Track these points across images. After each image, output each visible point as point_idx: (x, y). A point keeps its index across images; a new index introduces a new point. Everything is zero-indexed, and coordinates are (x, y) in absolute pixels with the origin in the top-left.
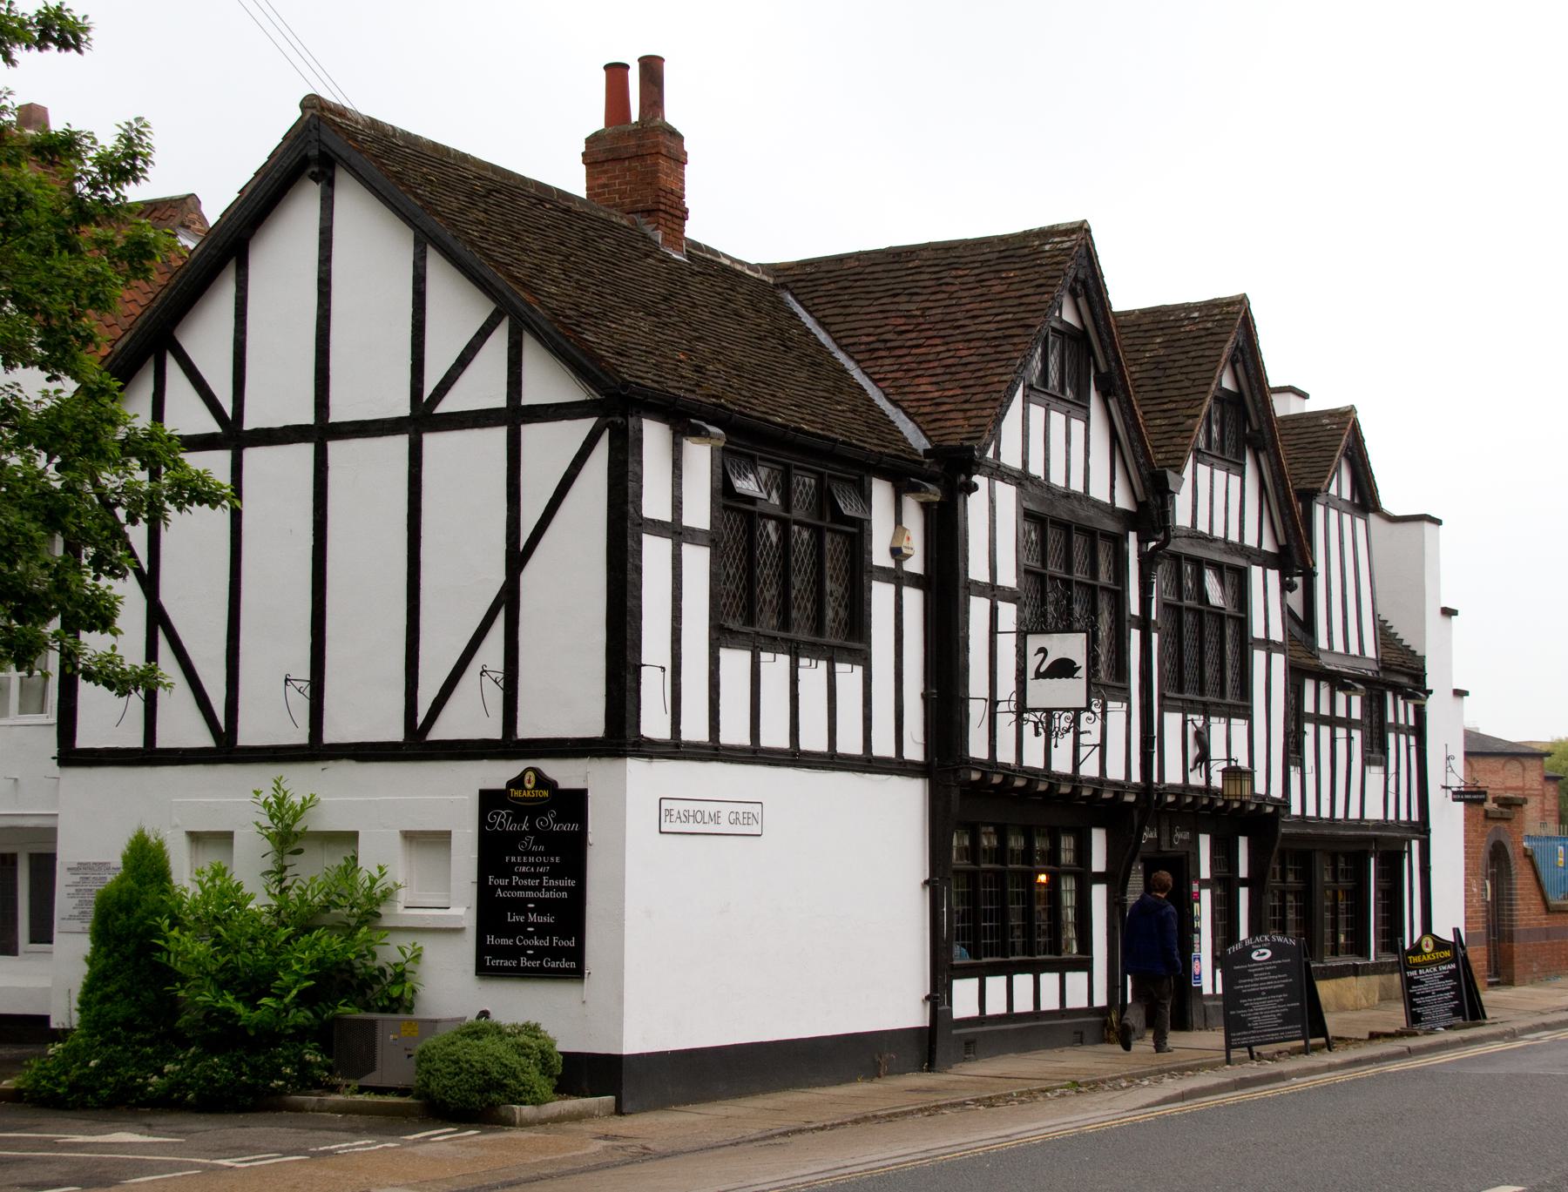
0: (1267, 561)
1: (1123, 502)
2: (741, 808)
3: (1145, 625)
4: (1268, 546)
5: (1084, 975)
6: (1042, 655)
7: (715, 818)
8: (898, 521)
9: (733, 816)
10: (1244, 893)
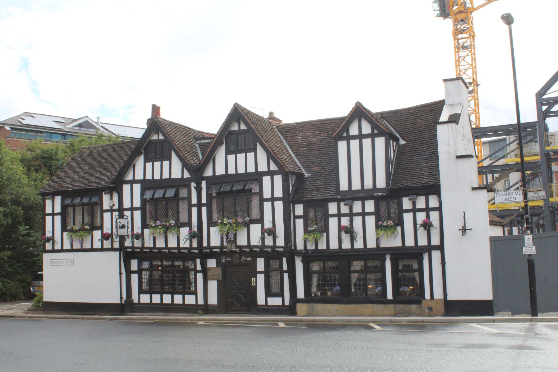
0: (271, 174)
1: (187, 175)
2: (68, 260)
3: (199, 205)
4: (273, 167)
5: (194, 296)
6: (120, 223)
7: (62, 262)
8: (111, 199)
9: (66, 262)
10: (286, 276)
